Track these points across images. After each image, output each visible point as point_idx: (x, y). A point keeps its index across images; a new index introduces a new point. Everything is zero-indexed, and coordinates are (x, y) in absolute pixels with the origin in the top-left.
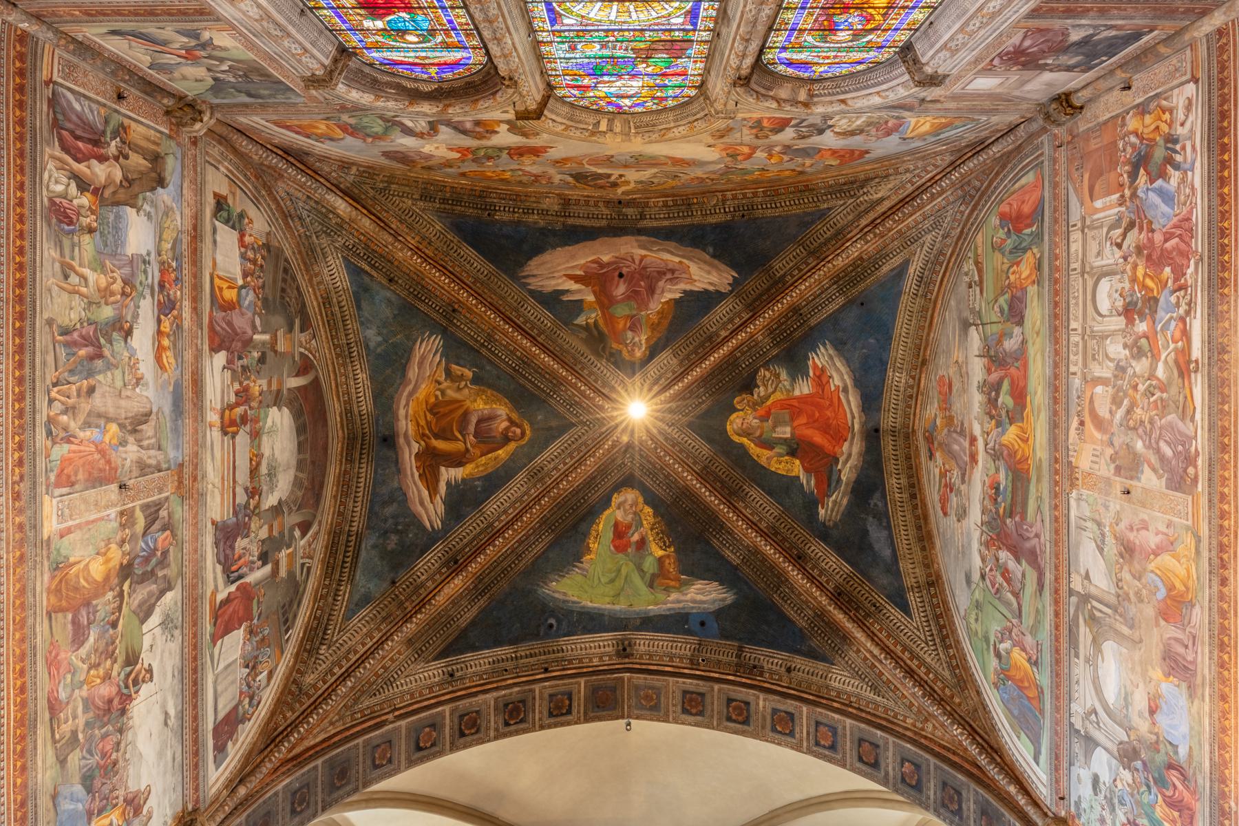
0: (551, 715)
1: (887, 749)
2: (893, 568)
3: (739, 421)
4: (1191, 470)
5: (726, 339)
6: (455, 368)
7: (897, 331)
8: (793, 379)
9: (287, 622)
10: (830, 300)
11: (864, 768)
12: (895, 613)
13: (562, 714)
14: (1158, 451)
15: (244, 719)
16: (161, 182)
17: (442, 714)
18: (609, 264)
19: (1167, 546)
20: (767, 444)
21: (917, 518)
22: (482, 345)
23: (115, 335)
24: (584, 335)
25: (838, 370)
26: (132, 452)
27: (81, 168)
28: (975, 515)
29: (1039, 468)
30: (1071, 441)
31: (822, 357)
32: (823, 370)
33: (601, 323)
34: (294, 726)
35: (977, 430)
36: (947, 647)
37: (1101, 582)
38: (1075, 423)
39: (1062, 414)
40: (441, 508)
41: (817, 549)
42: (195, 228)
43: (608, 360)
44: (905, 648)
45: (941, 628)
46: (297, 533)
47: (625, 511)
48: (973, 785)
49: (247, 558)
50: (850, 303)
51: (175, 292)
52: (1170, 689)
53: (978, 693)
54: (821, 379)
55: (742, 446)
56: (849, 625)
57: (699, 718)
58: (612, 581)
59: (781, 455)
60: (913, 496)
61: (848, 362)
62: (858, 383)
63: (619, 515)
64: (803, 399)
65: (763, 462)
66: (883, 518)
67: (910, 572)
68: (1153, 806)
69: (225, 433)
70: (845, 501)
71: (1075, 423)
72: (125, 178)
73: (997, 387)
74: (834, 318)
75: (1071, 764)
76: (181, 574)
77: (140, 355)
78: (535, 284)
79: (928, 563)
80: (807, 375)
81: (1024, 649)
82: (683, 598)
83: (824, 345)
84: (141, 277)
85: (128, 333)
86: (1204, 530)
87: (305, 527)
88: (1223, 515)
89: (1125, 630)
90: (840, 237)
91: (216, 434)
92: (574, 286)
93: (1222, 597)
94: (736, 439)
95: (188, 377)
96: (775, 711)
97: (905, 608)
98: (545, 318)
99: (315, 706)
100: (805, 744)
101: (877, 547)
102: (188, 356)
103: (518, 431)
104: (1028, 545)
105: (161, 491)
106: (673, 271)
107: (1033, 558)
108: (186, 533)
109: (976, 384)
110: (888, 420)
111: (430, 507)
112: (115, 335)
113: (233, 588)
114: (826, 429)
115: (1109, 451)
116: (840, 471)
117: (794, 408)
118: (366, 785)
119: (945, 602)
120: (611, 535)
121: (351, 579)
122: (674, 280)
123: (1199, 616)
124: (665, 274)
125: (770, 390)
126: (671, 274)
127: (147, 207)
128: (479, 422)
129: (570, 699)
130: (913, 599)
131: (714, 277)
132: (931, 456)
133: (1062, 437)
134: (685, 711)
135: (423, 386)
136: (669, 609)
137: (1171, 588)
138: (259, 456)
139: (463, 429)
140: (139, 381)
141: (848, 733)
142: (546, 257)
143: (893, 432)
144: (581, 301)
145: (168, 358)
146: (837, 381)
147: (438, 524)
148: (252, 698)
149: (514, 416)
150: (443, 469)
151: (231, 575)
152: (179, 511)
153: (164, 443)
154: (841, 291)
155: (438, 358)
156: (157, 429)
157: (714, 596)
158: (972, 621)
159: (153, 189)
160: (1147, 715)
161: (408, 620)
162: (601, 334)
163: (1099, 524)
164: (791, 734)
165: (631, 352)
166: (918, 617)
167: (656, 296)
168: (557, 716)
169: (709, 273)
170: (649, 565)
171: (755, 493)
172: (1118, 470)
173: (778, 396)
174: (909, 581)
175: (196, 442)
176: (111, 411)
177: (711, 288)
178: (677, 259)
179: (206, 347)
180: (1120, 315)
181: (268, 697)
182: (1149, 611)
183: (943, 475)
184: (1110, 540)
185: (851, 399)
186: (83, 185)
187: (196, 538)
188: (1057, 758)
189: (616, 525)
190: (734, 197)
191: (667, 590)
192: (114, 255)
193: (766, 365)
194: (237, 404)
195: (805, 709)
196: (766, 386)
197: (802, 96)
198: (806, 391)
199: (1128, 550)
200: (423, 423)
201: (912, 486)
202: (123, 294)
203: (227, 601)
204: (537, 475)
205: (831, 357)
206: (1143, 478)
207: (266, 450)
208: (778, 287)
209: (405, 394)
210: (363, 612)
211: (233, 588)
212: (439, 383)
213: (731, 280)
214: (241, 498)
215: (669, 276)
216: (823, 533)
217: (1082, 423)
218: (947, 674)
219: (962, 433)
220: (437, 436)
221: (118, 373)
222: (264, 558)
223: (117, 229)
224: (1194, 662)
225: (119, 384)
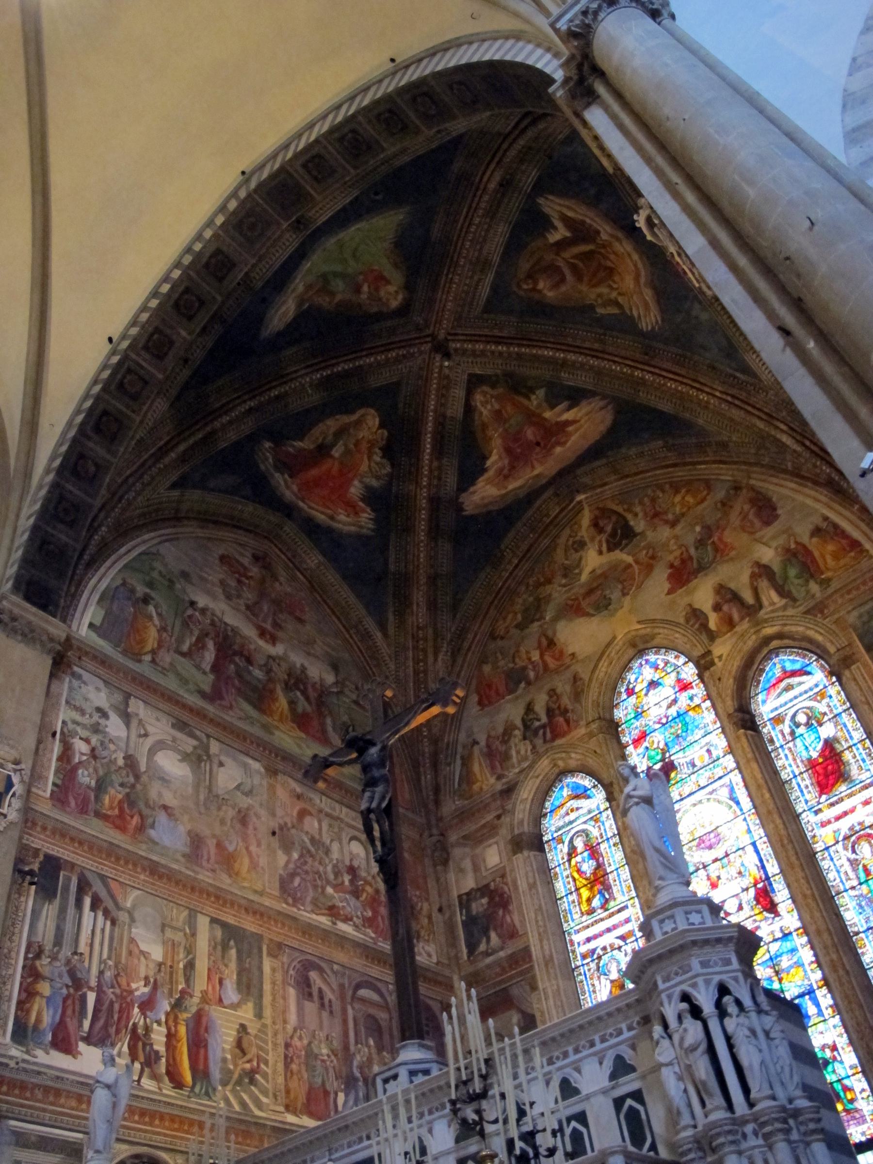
0: (319, 156)
1: (109, 451)
3: (370, 423)
5: (431, 461)
6: (615, 311)
8: (368, 488)
11: (98, 412)
13: (308, 161)
18: (553, 447)
20: (340, 433)
22: (605, 335)
24: (530, 383)
25: (350, 524)
30: (290, 781)
31: (366, 518)
32: (356, 513)
33: (525, 402)
40: (547, 210)
41: (247, 427)
43: (496, 375)
44: (153, 478)
47: (390, 293)
54: (351, 507)
55: (352, 412)
57: (204, 260)
58: (356, 249)
59: (324, 439)
61: (349, 535)
62: (330, 530)
63: (392, 289)
65: (330, 422)
67: (194, 497)
70: (262, 467)
71: (299, 790)
78: (597, 403)
80: (362, 500)
82: (294, 295)
83: (373, 530)
90: (433, 606)
92: (566, 416)
94: (362, 411)
96: (171, 343)
97: (174, 486)
98: (568, 379)
100: (134, 356)
103: (525, 287)
106: (506, 477)
109: (306, 664)
110: (289, 529)
111: (558, 208)
116: (283, 474)
120: (386, 274)
122: (500, 471)
124: (510, 470)
125: (373, 464)
126: (505, 475)
128: (563, 280)
129: (316, 179)
130: (176, 493)
131: (476, 498)
134: (218, 252)
135: (632, 286)
136: (295, 278)
139: (574, 268)
141: (129, 413)
142: (603, 428)
144: (552, 407)
146: (342, 517)
147: (541, 201)
149: (537, 296)
150: (568, 234)
155: (635, 313)
157: (276, 321)
160: (162, 802)
162: (519, 393)
164: (146, 348)
165: (485, 394)
167: (502, 450)
168: (313, 157)
169: (483, 498)
170: (339, 285)
171: (314, 398)
173: (364, 467)
177: (472, 489)
178: (511, 487)
180: (351, 860)
185: (323, 517)
189: (388, 282)
190: (510, 562)
191: (309, 287)
193: (391, 476)
195: (160, 376)
196: (377, 464)
197: (561, 763)
198: (353, 490)
200: (612, 257)
204: (483, 265)
205: (361, 527)
208: (435, 531)
209: (643, 273)
212: (620, 294)
213: (465, 507)
215: (506, 471)
216: (253, 439)
220: (591, 252)
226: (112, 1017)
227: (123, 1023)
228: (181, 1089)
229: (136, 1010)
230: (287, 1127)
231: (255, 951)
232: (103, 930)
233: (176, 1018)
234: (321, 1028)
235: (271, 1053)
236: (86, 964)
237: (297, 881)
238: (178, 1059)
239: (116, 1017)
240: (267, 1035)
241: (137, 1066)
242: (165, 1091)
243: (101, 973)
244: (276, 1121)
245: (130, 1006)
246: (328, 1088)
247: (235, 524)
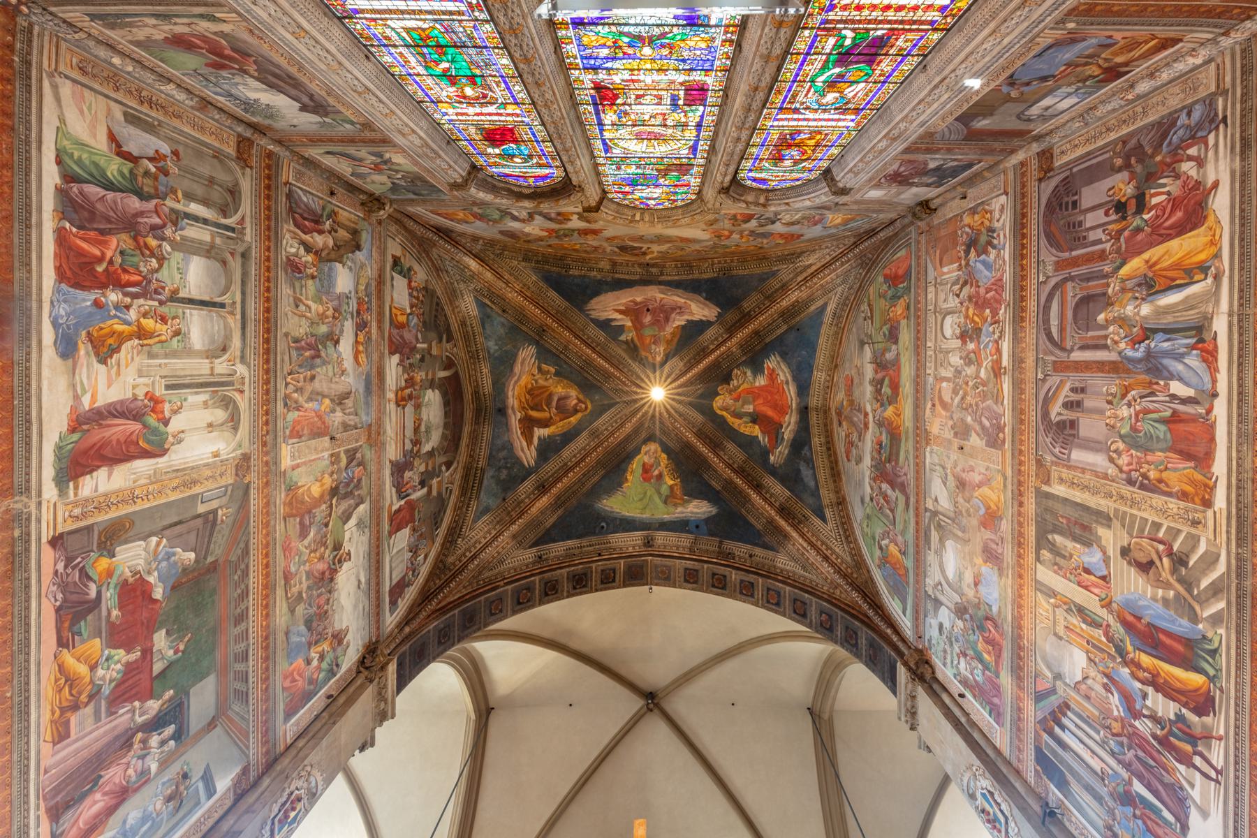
2: (816, 493)
4: (1001, 435)
7: (819, 347)
8: (755, 375)
9: (436, 523)
10: (778, 327)
12: (817, 521)
14: (981, 423)
15: (409, 584)
16: (358, 247)
17: (534, 582)
19: (986, 482)
21: (831, 462)
23: (328, 343)
26: (338, 417)
27: (307, 238)
28: (867, 461)
29: (907, 433)
31: (772, 362)
32: (773, 370)
34: (441, 588)
35: (869, 408)
36: (849, 543)
37: (945, 504)
38: (929, 405)
39: (922, 399)
42: (380, 276)
44: (823, 543)
45: (845, 531)
46: (444, 468)
48: (865, 629)
49: (412, 484)
50: (790, 329)
51: (367, 317)
52: (987, 570)
53: (868, 571)
54: (772, 376)
56: (788, 529)
60: (829, 449)
61: (789, 365)
62: (795, 378)
64: (761, 388)
66: (810, 462)
67: (827, 496)
68: (976, 643)
69: (398, 405)
71: (929, 405)
72: (335, 244)
73: (881, 382)
74: (780, 338)
75: (926, 616)
76: (370, 493)
77: (344, 356)
79: (838, 490)
81: (896, 544)
84: (345, 307)
85: (337, 342)
86: (1009, 472)
87: (448, 465)
88: (1021, 463)
89: (960, 534)
91: (393, 406)
93: (1020, 514)
95: (374, 370)
97: (823, 518)
99: (454, 576)
101: (806, 480)
102: (375, 357)
104: (899, 480)
105: (357, 441)
107: (903, 488)
108: (372, 467)
110: (814, 402)
112: (328, 343)
113: (402, 502)
114: (775, 407)
115: (951, 423)
117: (754, 394)
118: (486, 625)
119: (848, 515)
121: (478, 497)
123: (1006, 526)
127: (349, 263)
132: (840, 424)
133: (921, 413)
137: (988, 508)
138: (420, 420)
140: (343, 372)
143: (817, 409)
145: (362, 358)
146: (782, 377)
148: (414, 571)
151: (401, 494)
152: (369, 454)
153: (359, 411)
154: (785, 321)
156: (355, 402)
158: (865, 526)
159: (353, 252)
161: (513, 522)
163: (944, 468)
166: (831, 524)
172: (956, 434)
173: (745, 386)
174: (826, 502)
175: (380, 411)
176: (326, 391)
179: (387, 352)
181: (424, 571)
182: (975, 522)
183: (847, 436)
184: (950, 477)
186: (308, 249)
187: (379, 471)
188: (917, 612)
192: (328, 293)
193: (738, 367)
194: (406, 388)
198: (763, 383)
199: (962, 484)
201: (828, 442)
202: (334, 317)
203: (399, 510)
206: (972, 439)
207: (424, 417)
210: (485, 518)
211: (402, 502)
214: (408, 446)
216: (773, 471)
217: (934, 405)
218: (849, 559)
219: (859, 410)
221: (330, 367)
222: (423, 483)
223: (330, 276)
224: (1002, 554)
225: (331, 374)
226: (1152, 767)
227: (1155, 754)
228: (1213, 699)
229: (1137, 723)
230: (1234, 511)
231: (1050, 503)
232: (1077, 725)
233: (1132, 661)
234: (1101, 412)
235: (1145, 515)
236: (1110, 772)
237: (987, 423)
238: (1178, 685)
239: (1153, 763)
240: (1125, 513)
241: (1197, 760)
242: (1222, 732)
243: (1113, 754)
244: (1228, 532)
245: (1135, 735)
246: (1168, 413)
247: (829, 445)
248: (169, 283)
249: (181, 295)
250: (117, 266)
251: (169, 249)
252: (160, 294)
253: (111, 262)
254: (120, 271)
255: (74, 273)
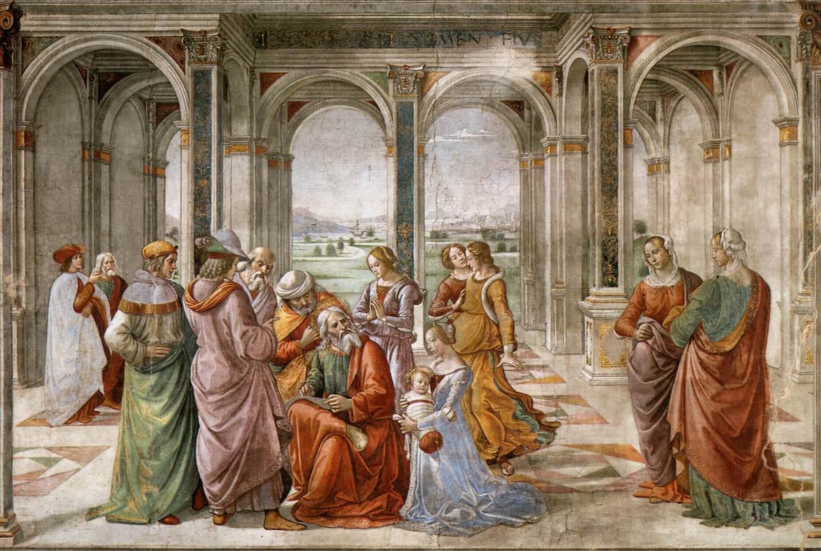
248: (368, 277)
249: (386, 235)
250: (348, 404)
251: (289, 278)
252: (396, 300)
253: (343, 416)
254: (358, 398)
255: (376, 493)
